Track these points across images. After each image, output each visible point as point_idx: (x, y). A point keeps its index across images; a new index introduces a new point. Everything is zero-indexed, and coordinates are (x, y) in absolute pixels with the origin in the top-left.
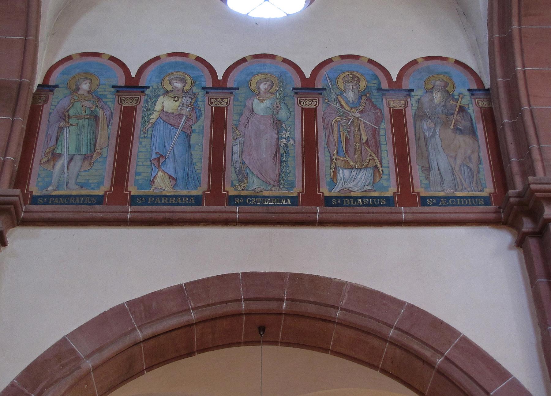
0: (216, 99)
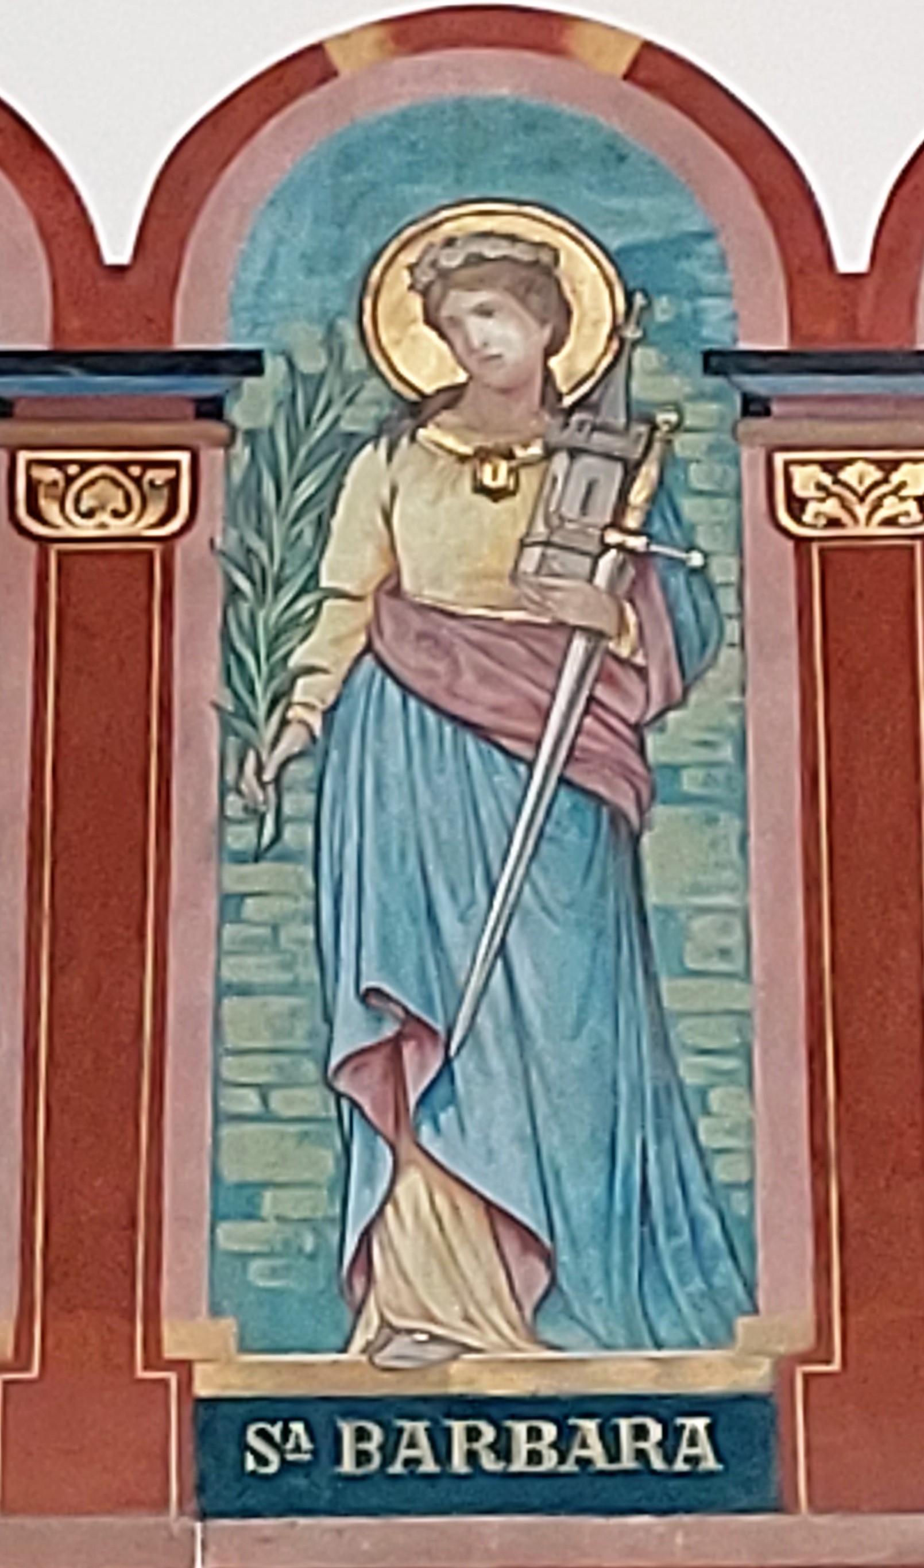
0: (832, 467)
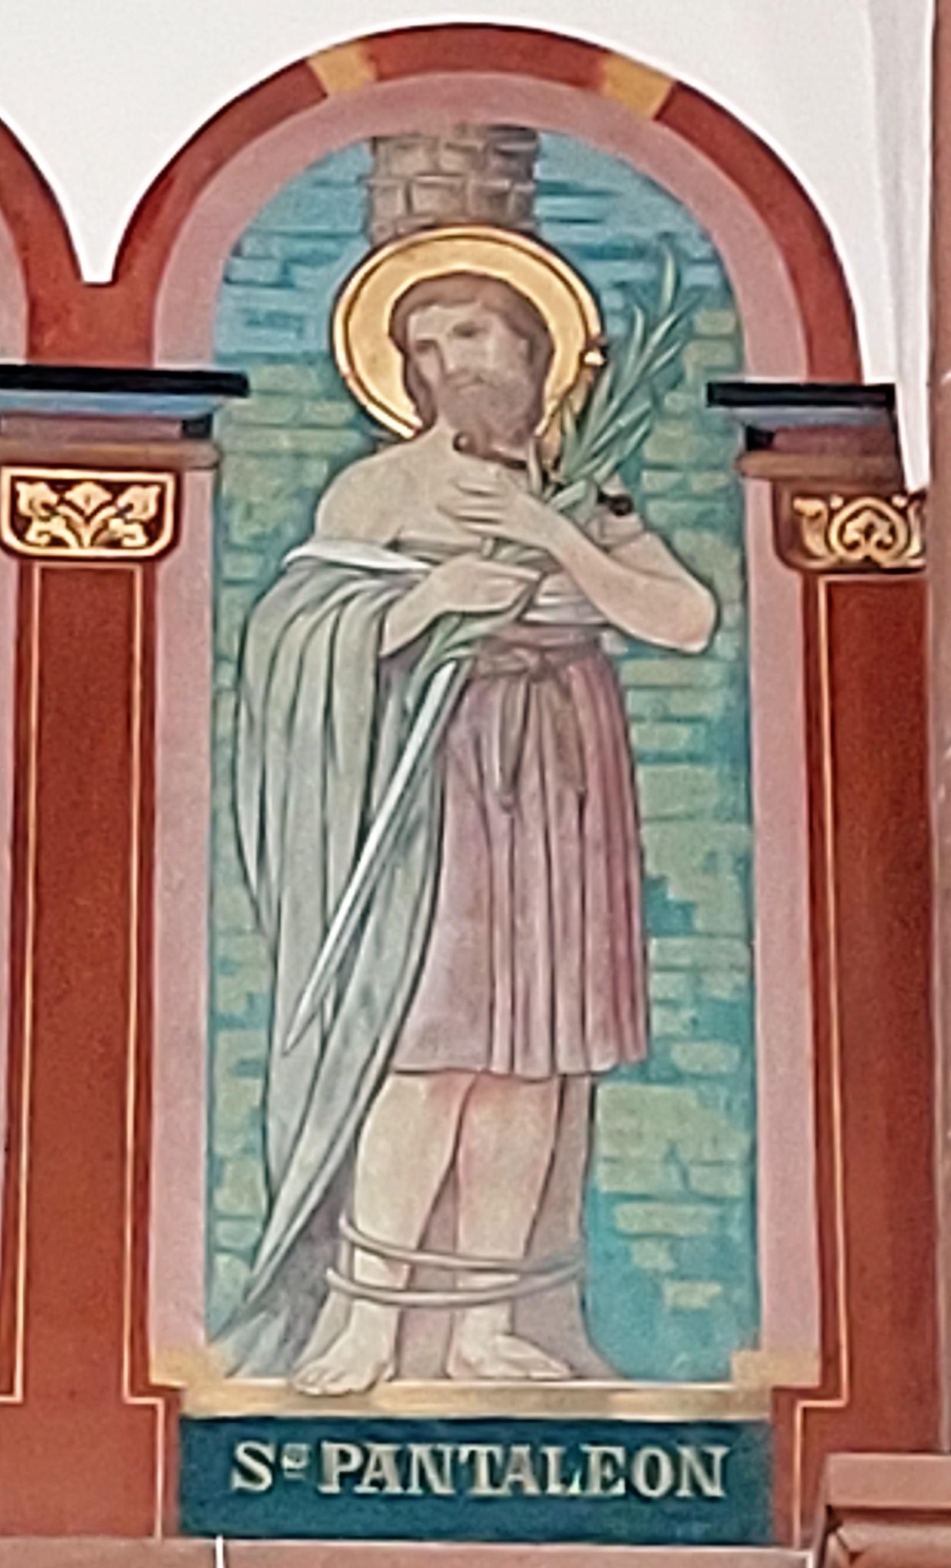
0: (60, 487)
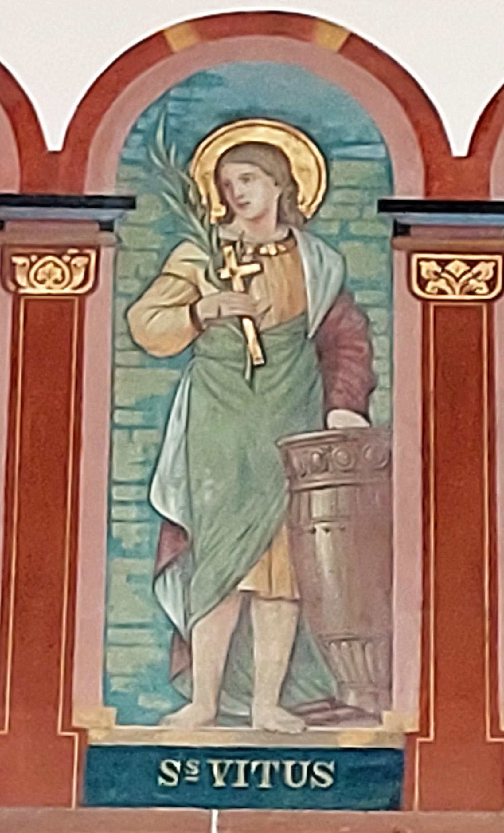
0: (443, 263)
